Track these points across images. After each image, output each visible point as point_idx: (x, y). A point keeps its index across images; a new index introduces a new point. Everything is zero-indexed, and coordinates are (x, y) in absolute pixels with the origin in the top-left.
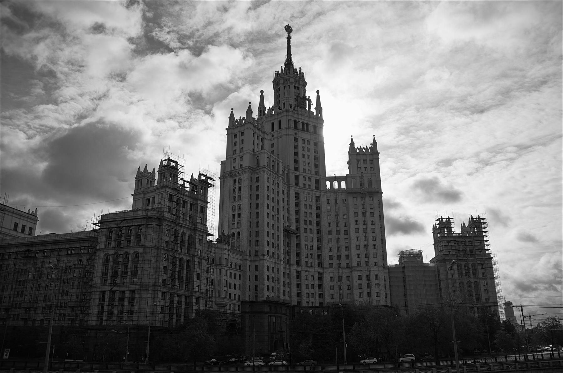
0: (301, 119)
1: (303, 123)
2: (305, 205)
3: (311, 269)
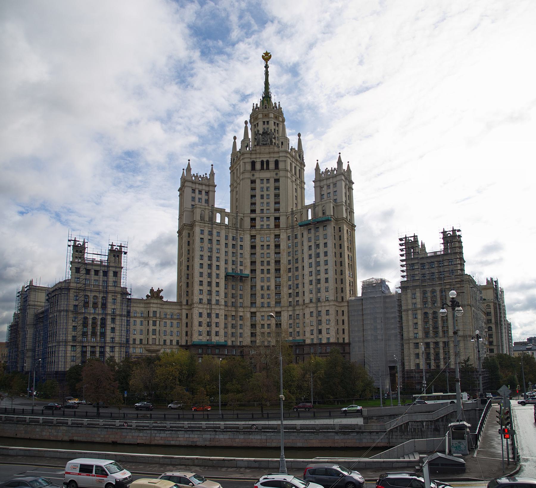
0: (260, 158)
1: (262, 162)
2: (262, 246)
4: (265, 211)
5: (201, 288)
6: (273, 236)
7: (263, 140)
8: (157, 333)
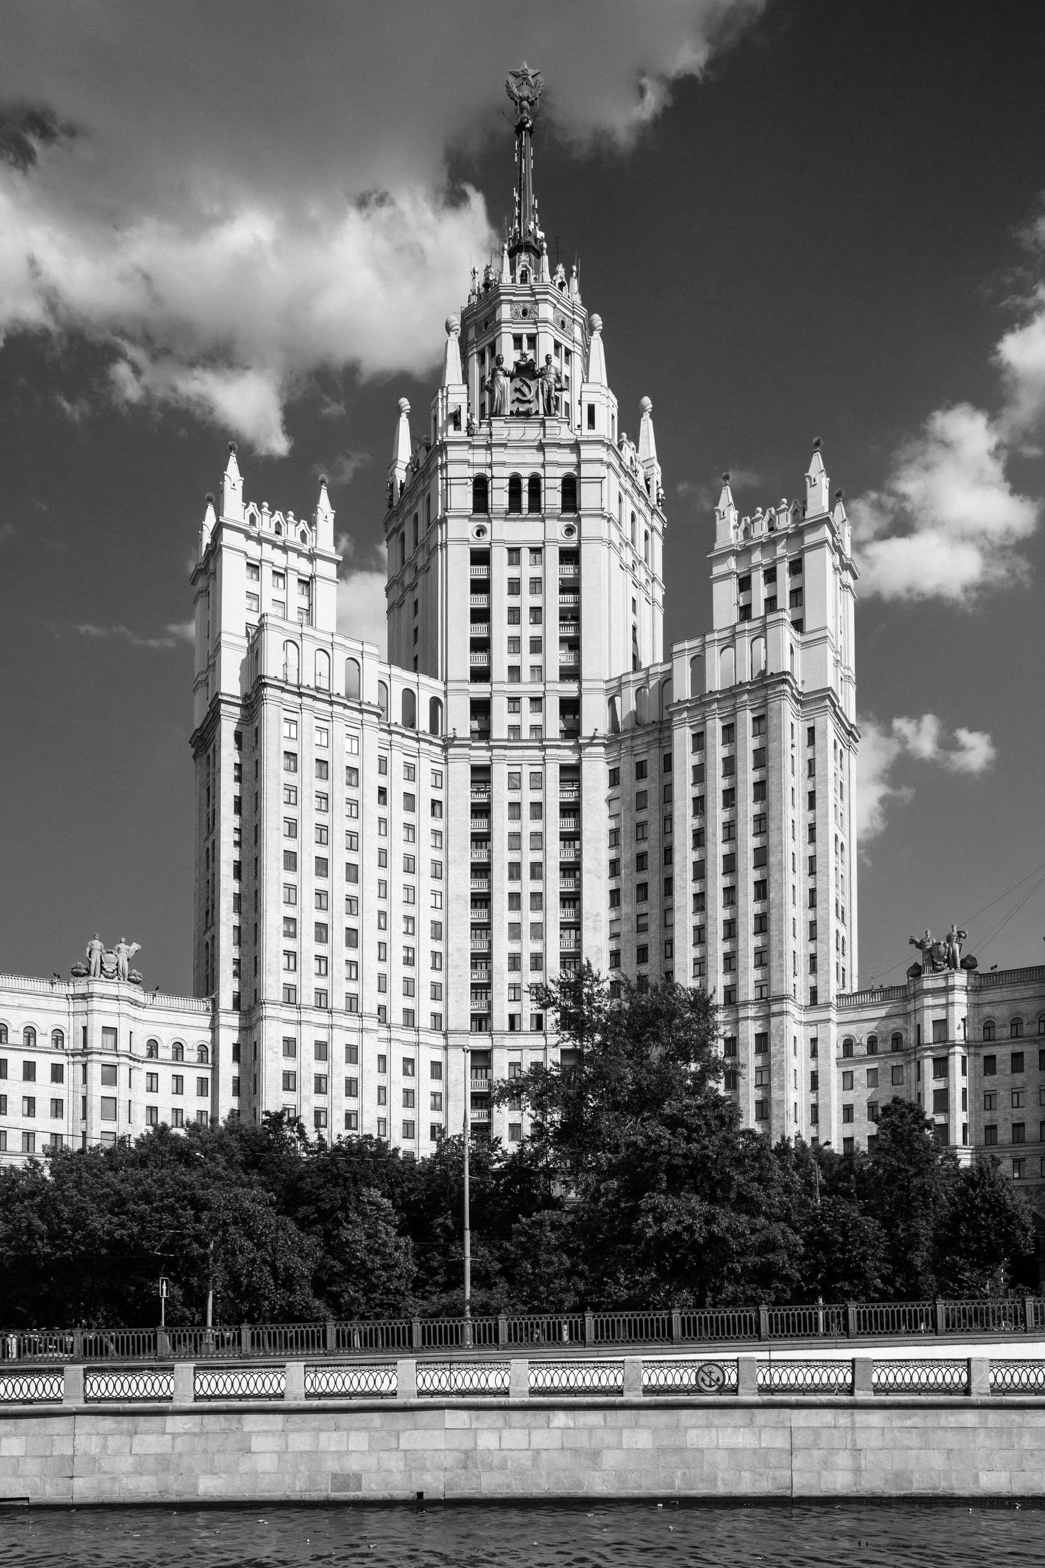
5: (290, 945)
7: (518, 395)
8: (122, 1112)
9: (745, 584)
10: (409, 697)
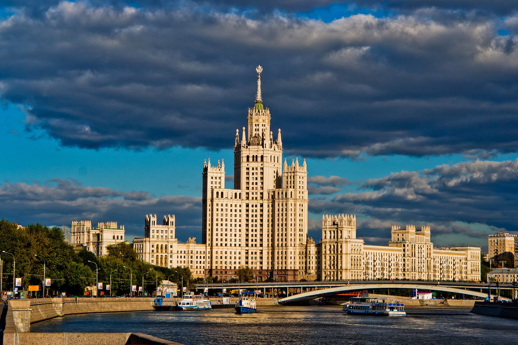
3: (256, 248)
4: (255, 188)
5: (217, 237)
6: (259, 206)
9: (287, 177)
10: (236, 194)
